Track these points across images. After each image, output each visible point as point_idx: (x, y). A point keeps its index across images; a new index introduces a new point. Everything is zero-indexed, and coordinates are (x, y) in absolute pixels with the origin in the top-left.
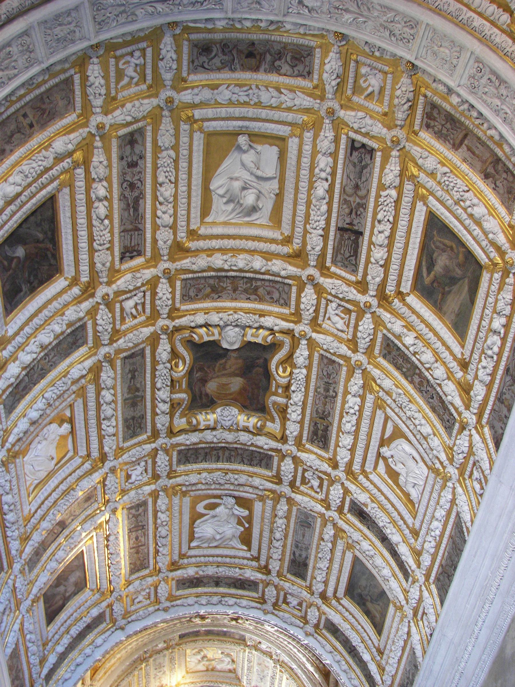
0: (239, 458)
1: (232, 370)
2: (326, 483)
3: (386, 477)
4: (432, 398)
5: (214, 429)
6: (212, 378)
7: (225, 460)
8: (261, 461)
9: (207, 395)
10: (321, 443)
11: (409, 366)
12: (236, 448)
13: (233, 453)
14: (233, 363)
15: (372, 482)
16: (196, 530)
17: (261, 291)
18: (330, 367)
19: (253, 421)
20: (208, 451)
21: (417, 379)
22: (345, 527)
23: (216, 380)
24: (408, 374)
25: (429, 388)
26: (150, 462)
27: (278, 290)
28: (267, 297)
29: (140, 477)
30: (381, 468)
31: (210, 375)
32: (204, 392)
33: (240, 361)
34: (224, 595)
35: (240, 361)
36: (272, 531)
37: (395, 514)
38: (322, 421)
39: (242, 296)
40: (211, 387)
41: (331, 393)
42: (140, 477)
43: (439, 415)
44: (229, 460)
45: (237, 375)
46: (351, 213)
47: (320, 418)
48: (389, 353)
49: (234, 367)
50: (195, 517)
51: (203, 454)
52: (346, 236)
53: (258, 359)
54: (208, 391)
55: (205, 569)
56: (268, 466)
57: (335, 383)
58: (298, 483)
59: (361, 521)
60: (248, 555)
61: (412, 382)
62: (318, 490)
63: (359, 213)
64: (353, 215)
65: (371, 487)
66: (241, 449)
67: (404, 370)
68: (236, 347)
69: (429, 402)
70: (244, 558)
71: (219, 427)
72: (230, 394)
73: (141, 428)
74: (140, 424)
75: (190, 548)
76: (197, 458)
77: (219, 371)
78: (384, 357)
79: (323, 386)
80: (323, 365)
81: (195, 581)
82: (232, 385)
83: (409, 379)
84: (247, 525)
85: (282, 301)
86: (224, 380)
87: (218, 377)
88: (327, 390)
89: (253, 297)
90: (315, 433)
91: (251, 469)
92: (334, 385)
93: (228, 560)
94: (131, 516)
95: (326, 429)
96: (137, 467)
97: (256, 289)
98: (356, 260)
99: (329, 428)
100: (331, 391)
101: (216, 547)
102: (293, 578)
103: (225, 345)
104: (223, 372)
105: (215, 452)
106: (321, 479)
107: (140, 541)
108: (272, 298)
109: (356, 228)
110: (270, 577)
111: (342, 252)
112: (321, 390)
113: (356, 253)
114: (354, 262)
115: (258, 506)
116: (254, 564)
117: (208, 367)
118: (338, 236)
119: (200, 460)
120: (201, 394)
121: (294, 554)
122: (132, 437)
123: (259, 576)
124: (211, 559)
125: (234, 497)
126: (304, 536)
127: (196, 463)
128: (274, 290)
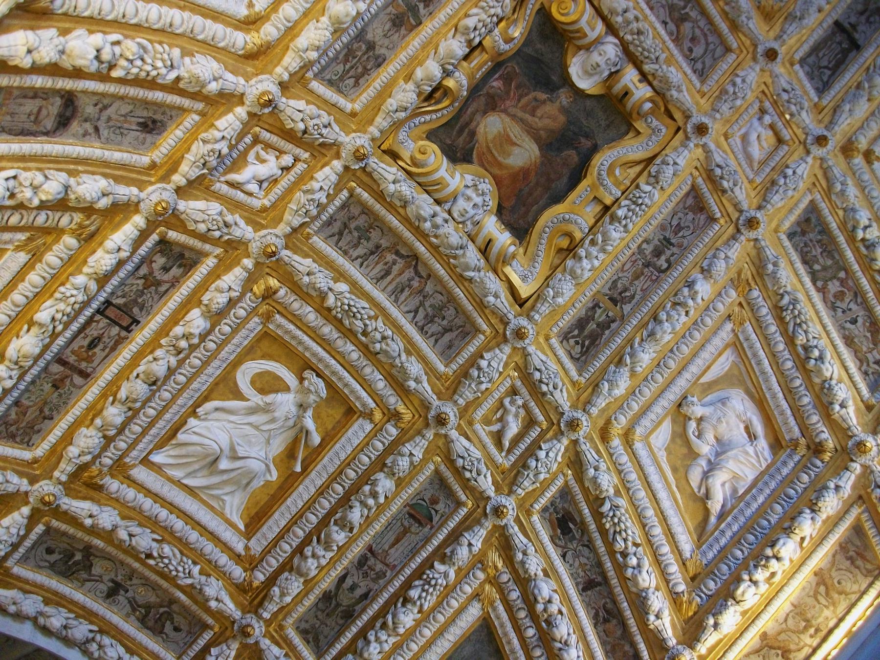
0: (415, 302)
1: (540, 125)
2: (534, 433)
3: (662, 456)
4: (854, 322)
5: (438, 202)
6: (505, 111)
7: (390, 288)
8: (446, 330)
9: (473, 134)
10: (578, 349)
11: (829, 262)
12: (431, 275)
13: (415, 284)
14: (551, 113)
15: (634, 456)
16: (192, 422)
17: (687, 27)
18: (690, 216)
19: (503, 239)
20: (384, 243)
21: (834, 287)
22: (520, 539)
23: (507, 119)
24: (821, 275)
25: (852, 305)
26: (300, 167)
27: (707, 44)
28: (687, 44)
29: (253, 187)
30: (662, 436)
31: (508, 103)
32: (474, 124)
33: (562, 119)
34: (107, 629)
35: (562, 119)
36: (345, 502)
37: (657, 531)
38: (610, 304)
39: (662, 10)
40: (491, 126)
41: (662, 262)
42: (253, 187)
43: (856, 353)
44: (396, 294)
45: (537, 139)
46: (862, 13)
47: (612, 299)
48: (804, 233)
49: (547, 121)
50: (224, 385)
51: (370, 245)
52: (838, 38)
53: (587, 136)
54: (481, 129)
55: (136, 530)
56: (448, 353)
57: (680, 246)
58: (479, 414)
59: (552, 539)
60: (240, 547)
61: (822, 290)
62: (507, 444)
63: (872, 19)
64: (863, 19)
65: (629, 466)
66: (440, 281)
67: (817, 267)
68: (584, 84)
69: (844, 328)
70: (226, 548)
71: (447, 206)
72: (500, 165)
73: (357, 84)
74: (366, 71)
75: (145, 461)
76: (356, 246)
77: (524, 109)
78: (791, 236)
79: (656, 242)
80: (681, 205)
81: (78, 557)
82: (516, 150)
83: (820, 284)
84: (298, 469)
85: (699, 66)
86: (515, 131)
87: (513, 117)
88: (657, 253)
89: (672, 26)
90: (581, 324)
91: (417, 338)
92: (675, 250)
93: (193, 536)
94: (144, 270)
95: (605, 326)
96: (271, 157)
97: (685, 18)
98: (830, 77)
99: (614, 326)
100: (663, 258)
101: (191, 491)
102: (297, 640)
103: (575, 69)
104: (527, 117)
105: (390, 257)
106: (530, 422)
107: (89, 359)
108: (691, 50)
109: (857, 36)
110: (251, 619)
111: (821, 55)
112: (648, 249)
113: (838, 67)
114: (825, 79)
115: (359, 430)
116: (238, 573)
117: (518, 87)
118: (829, 32)
119: (355, 254)
120: (467, 124)
121: (342, 579)
122: (331, 83)
123: (230, 607)
124: (163, 514)
125: (329, 385)
126: (393, 545)
127: (345, 253)
128: (703, 41)
